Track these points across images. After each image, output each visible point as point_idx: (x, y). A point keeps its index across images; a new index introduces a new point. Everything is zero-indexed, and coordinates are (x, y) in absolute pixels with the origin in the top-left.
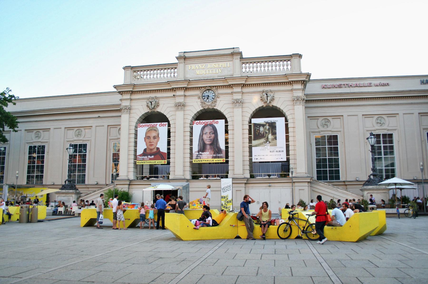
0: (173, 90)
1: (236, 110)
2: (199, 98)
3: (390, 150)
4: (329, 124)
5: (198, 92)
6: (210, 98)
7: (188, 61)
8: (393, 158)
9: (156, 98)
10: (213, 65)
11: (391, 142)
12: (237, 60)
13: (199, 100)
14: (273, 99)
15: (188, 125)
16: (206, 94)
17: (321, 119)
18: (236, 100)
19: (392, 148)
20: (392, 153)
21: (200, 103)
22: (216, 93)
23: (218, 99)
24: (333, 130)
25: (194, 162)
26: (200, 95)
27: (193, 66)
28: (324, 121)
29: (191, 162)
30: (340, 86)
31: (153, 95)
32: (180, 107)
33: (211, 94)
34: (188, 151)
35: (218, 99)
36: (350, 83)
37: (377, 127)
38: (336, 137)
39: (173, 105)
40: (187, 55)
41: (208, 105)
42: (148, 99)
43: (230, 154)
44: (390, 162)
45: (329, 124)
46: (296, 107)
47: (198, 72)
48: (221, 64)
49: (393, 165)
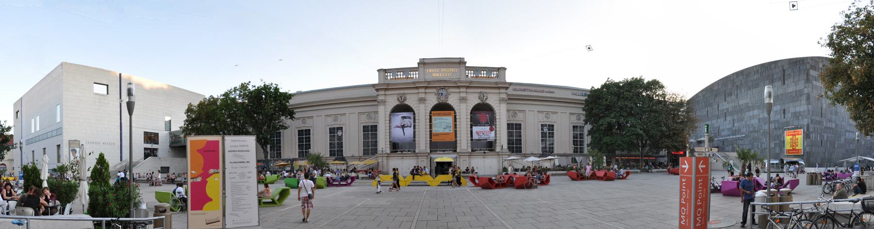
0: (417, 88)
1: (462, 104)
2: (436, 95)
3: (552, 135)
4: (516, 115)
5: (434, 90)
6: (444, 95)
7: (426, 66)
8: (553, 140)
9: (404, 94)
10: (445, 70)
11: (553, 130)
12: (463, 69)
13: (436, 96)
14: (487, 99)
15: (428, 114)
16: (441, 91)
17: (511, 112)
18: (462, 97)
19: (553, 133)
20: (553, 137)
21: (436, 99)
22: (448, 92)
23: (449, 96)
24: (519, 120)
25: (433, 141)
26: (436, 92)
27: (430, 70)
28: (513, 114)
29: (430, 141)
30: (524, 90)
31: (402, 92)
32: (422, 101)
33: (444, 92)
34: (429, 133)
35: (449, 96)
36: (531, 88)
37: (545, 120)
38: (520, 125)
39: (417, 99)
40: (425, 61)
41: (443, 99)
42: (398, 94)
43: (458, 136)
44: (551, 142)
45: (516, 115)
46: (502, 105)
47: (434, 75)
48: (451, 70)
49: (553, 144)
